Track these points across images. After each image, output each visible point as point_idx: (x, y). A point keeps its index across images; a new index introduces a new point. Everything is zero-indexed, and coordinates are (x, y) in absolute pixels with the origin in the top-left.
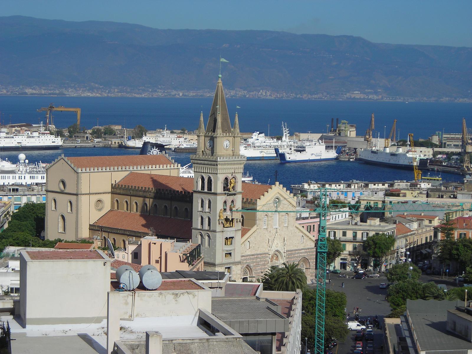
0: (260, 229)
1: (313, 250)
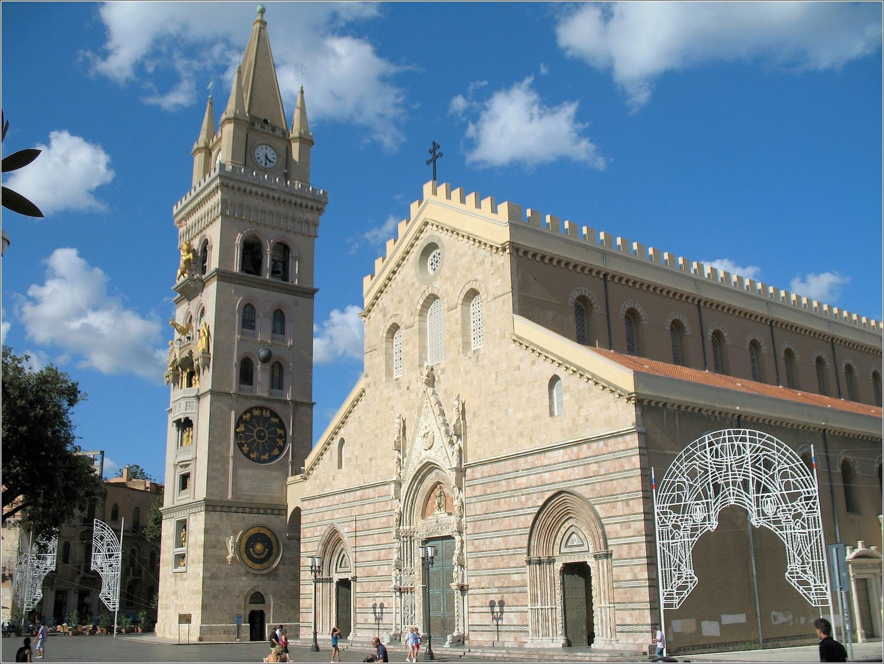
0: (375, 384)
1: (619, 444)
